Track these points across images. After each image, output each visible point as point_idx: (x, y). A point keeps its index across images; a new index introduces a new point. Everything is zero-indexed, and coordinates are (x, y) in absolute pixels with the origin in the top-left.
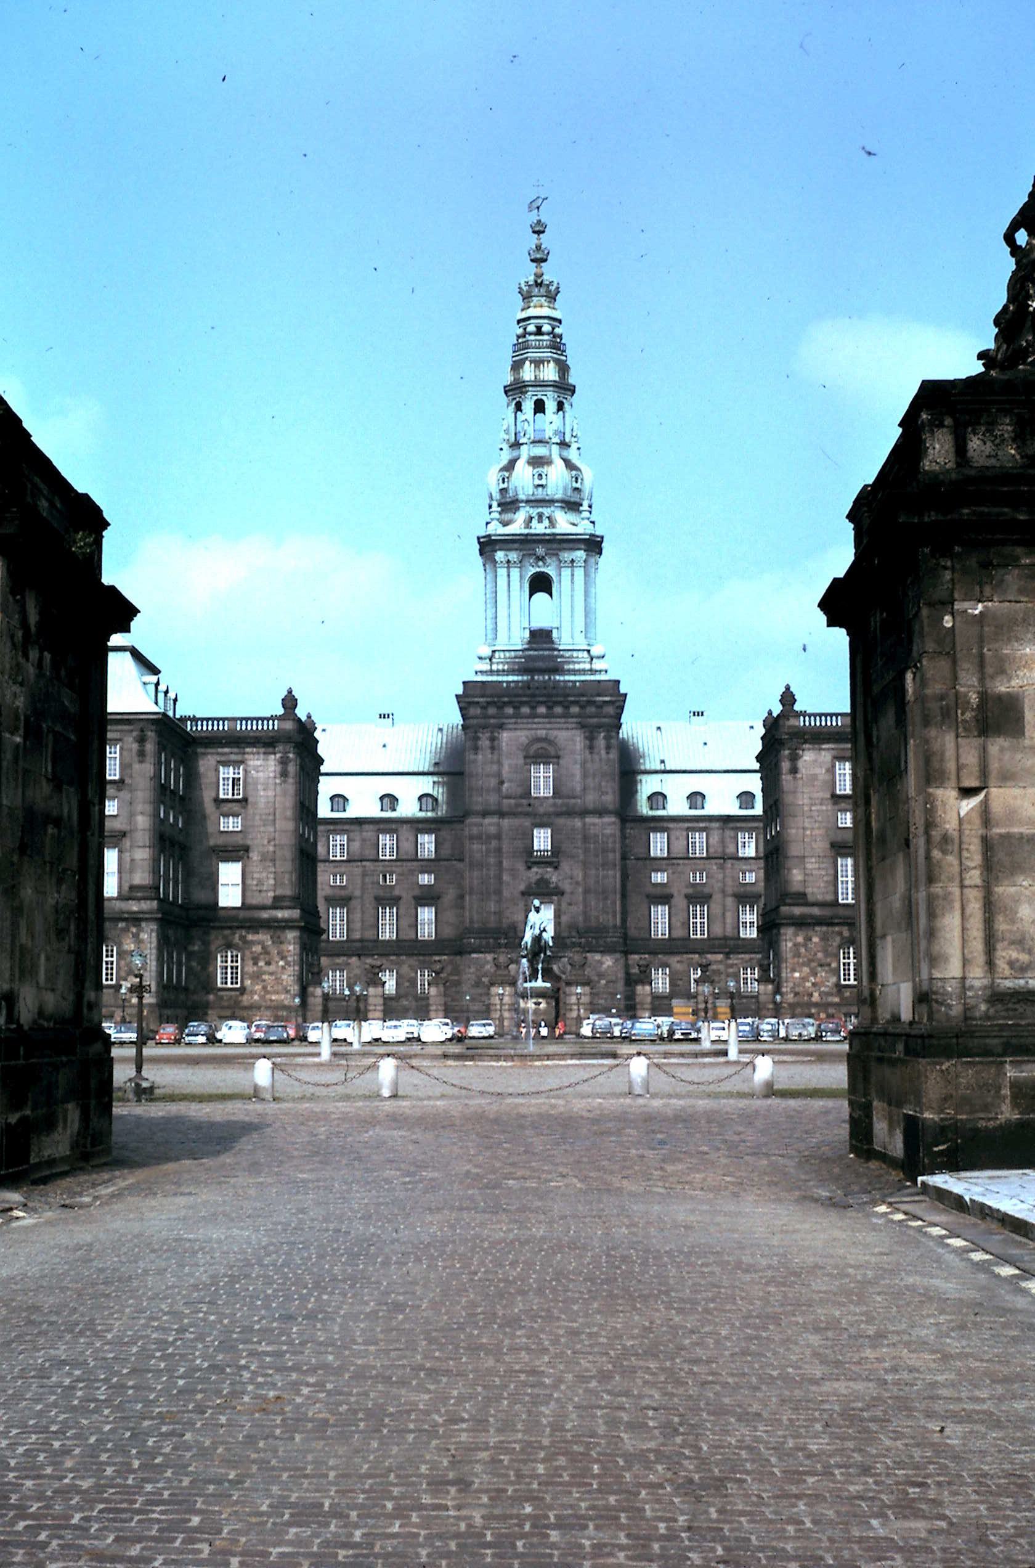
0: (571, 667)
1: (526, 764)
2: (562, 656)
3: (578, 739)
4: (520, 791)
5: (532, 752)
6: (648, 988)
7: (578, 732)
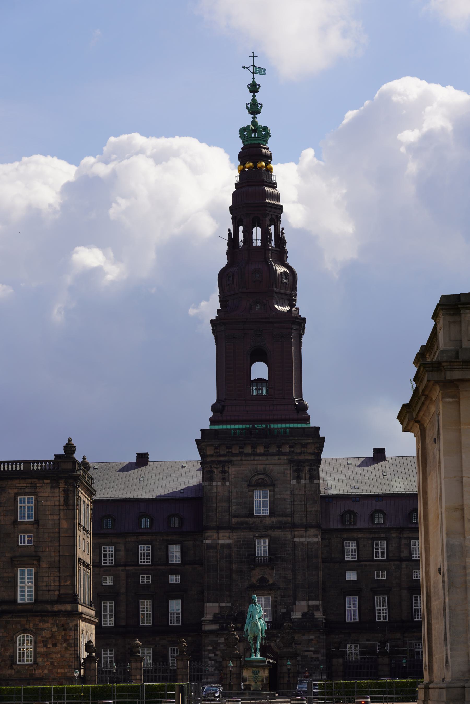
1: (249, 491)
3: (288, 472)
6: (340, 660)
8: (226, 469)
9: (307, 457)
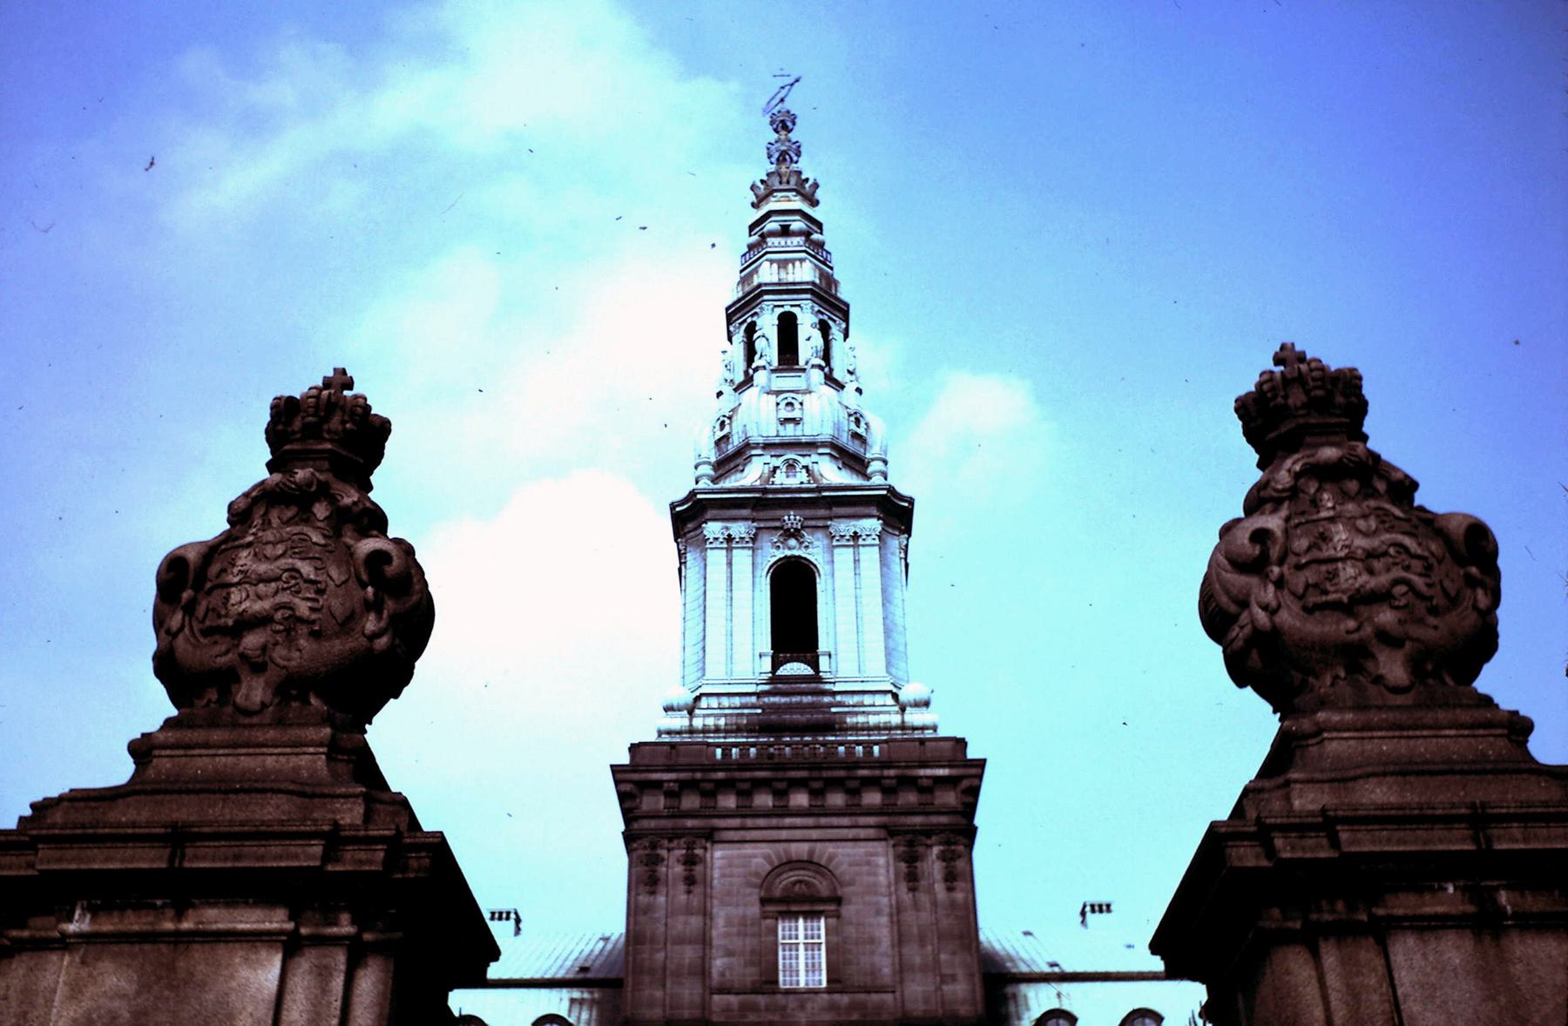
0: (861, 719)
1: (764, 916)
2: (840, 705)
3: (881, 861)
4: (751, 975)
5: (777, 893)
7: (879, 847)
8: (698, 852)
9: (935, 819)
